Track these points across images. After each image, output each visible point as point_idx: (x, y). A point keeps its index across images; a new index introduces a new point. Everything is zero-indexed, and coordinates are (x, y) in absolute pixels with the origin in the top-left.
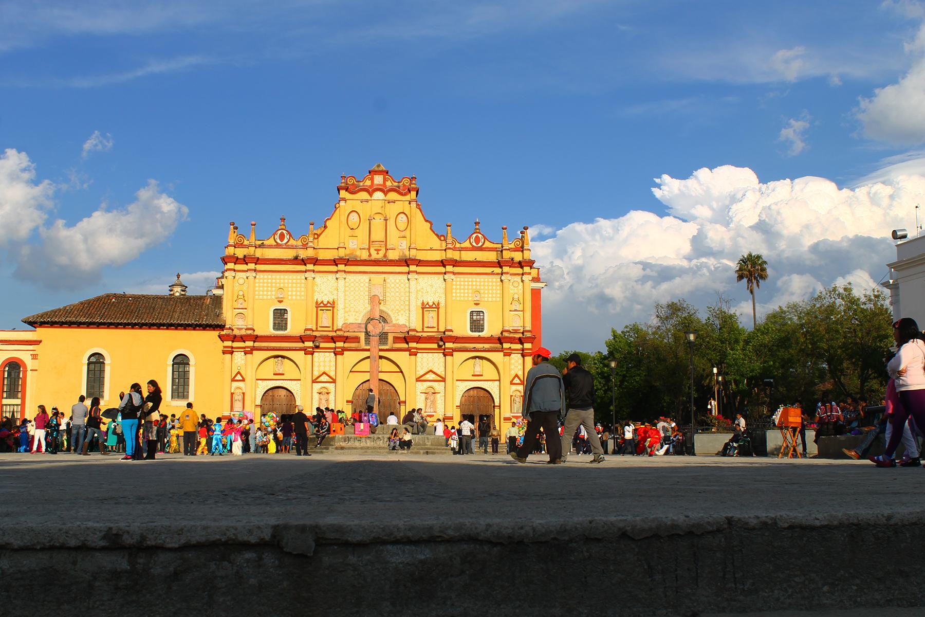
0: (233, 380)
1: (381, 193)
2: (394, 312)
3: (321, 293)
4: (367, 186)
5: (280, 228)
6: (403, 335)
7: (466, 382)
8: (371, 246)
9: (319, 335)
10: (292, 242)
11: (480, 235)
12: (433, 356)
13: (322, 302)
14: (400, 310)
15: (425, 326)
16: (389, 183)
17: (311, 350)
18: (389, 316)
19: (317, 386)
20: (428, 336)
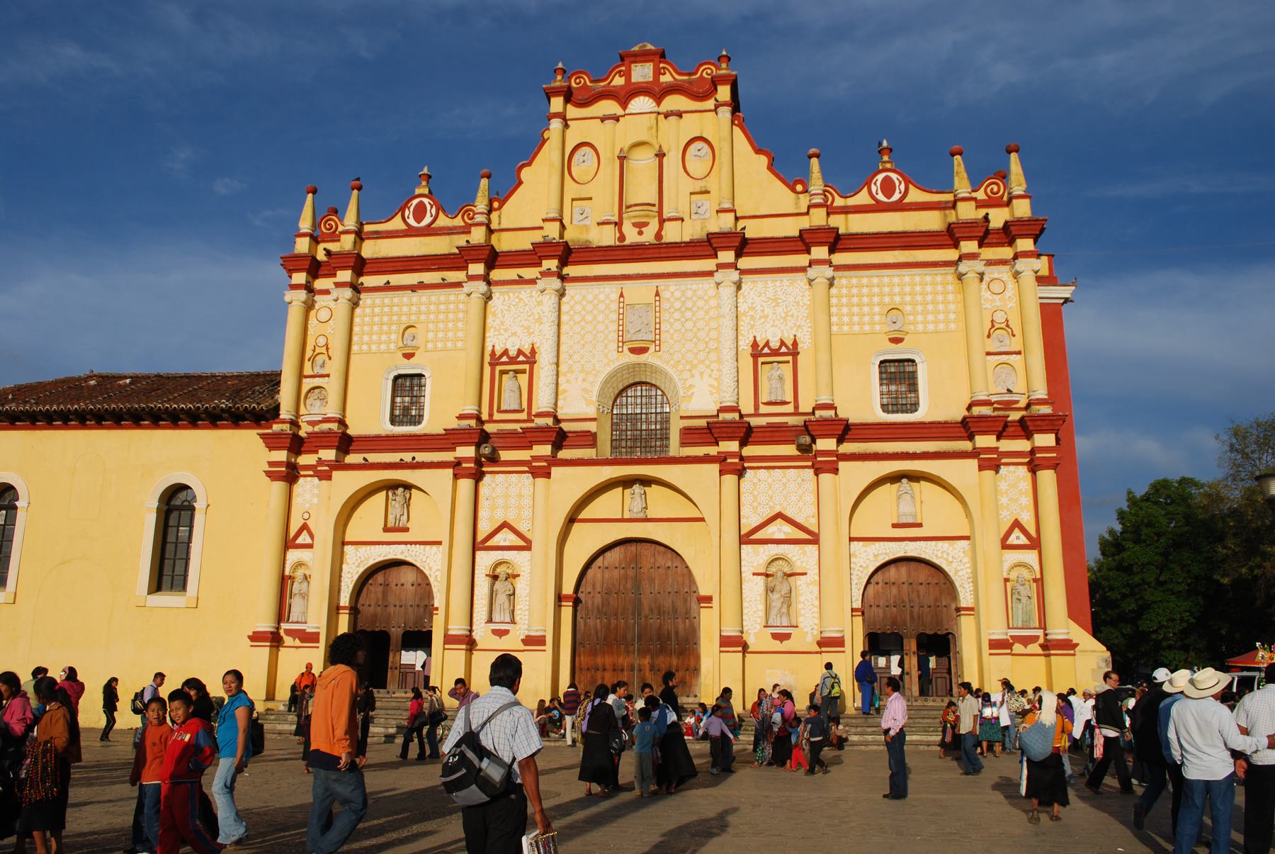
0: (288, 543)
1: (647, 98)
2: (681, 367)
3: (502, 331)
4: (613, 87)
5: (418, 191)
6: (703, 423)
7: (877, 544)
8: (624, 216)
9: (495, 431)
10: (443, 221)
11: (894, 176)
12: (785, 476)
13: (506, 352)
14: (695, 362)
15: (764, 397)
16: (666, 78)
17: (472, 465)
18: (671, 380)
19: (485, 560)
20: (770, 425)
